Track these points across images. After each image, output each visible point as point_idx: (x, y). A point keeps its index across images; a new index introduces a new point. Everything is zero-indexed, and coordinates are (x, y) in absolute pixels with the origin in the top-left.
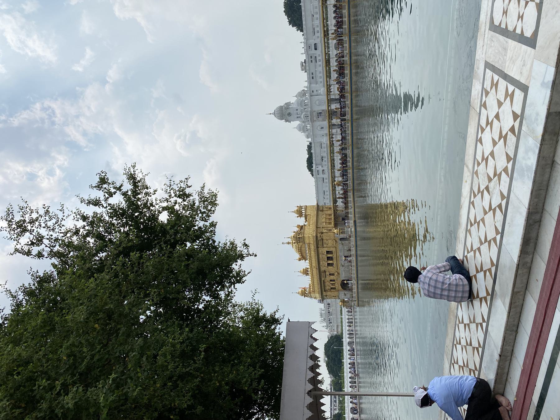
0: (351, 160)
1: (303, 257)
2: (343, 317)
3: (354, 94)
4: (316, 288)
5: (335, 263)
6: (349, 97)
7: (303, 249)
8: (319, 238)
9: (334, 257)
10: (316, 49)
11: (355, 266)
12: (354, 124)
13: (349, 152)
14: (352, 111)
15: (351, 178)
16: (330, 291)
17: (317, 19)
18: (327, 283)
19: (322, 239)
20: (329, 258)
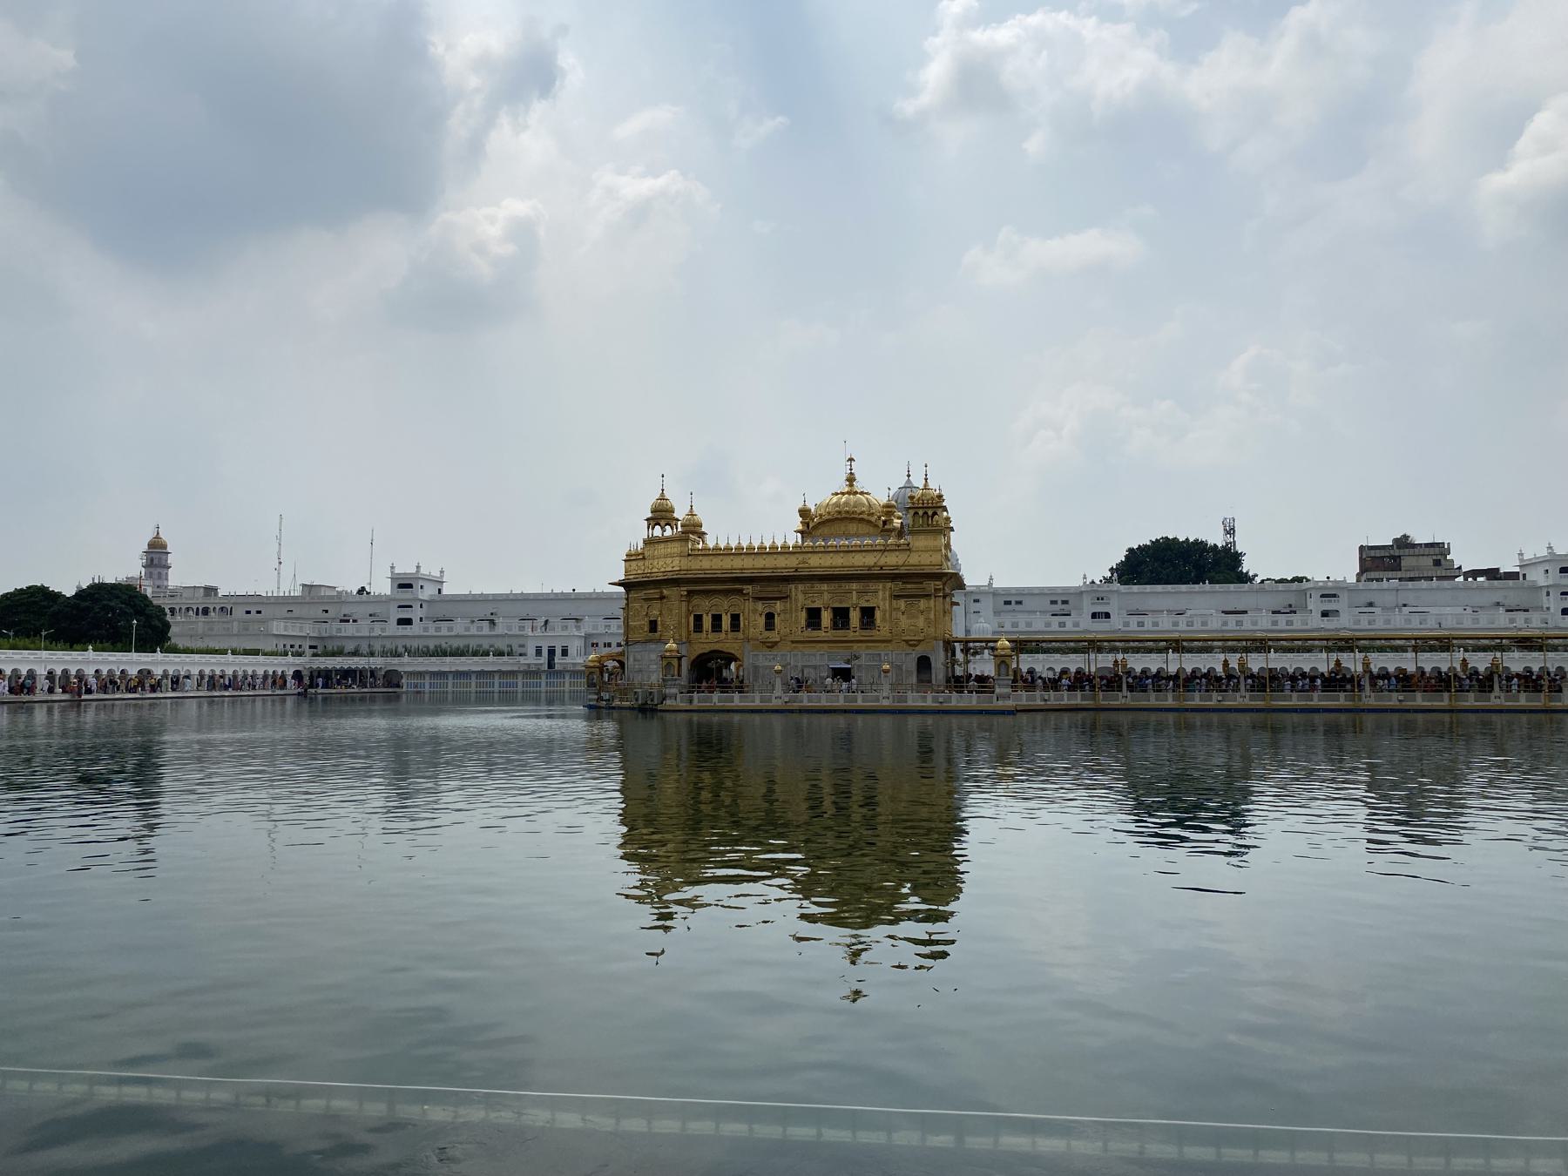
0: (1212, 703)
1: (812, 524)
2: (230, 657)
3: (1446, 717)
4: (706, 563)
5: (821, 634)
6: (1437, 704)
7: (853, 527)
8: (931, 586)
9: (850, 635)
10: (1094, 616)
11: (852, 706)
12: (1343, 717)
13: (1242, 698)
14: (1393, 711)
15: (1144, 704)
16: (689, 612)
17: (1176, 624)
18: (724, 606)
19: (927, 596)
20: (841, 616)
